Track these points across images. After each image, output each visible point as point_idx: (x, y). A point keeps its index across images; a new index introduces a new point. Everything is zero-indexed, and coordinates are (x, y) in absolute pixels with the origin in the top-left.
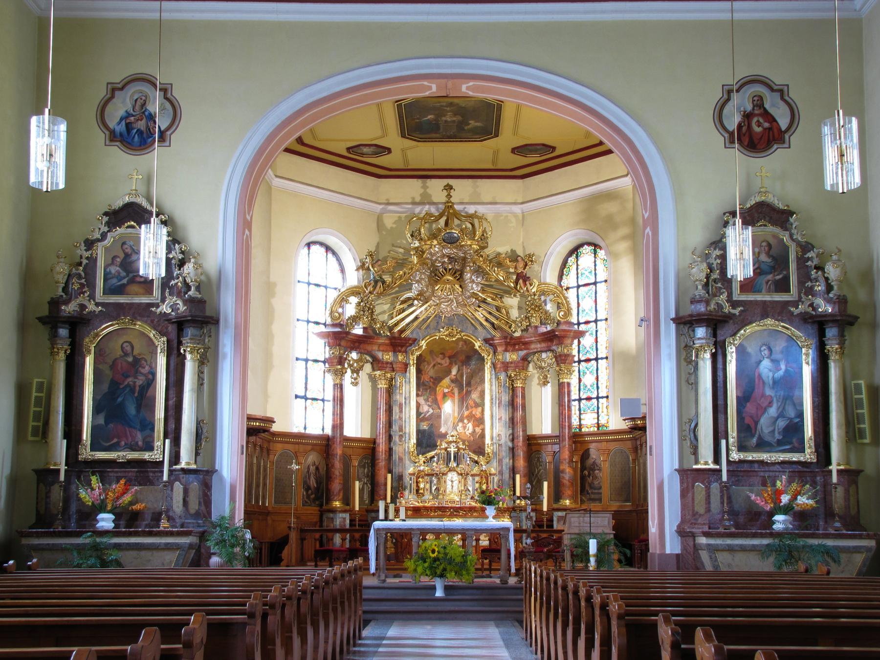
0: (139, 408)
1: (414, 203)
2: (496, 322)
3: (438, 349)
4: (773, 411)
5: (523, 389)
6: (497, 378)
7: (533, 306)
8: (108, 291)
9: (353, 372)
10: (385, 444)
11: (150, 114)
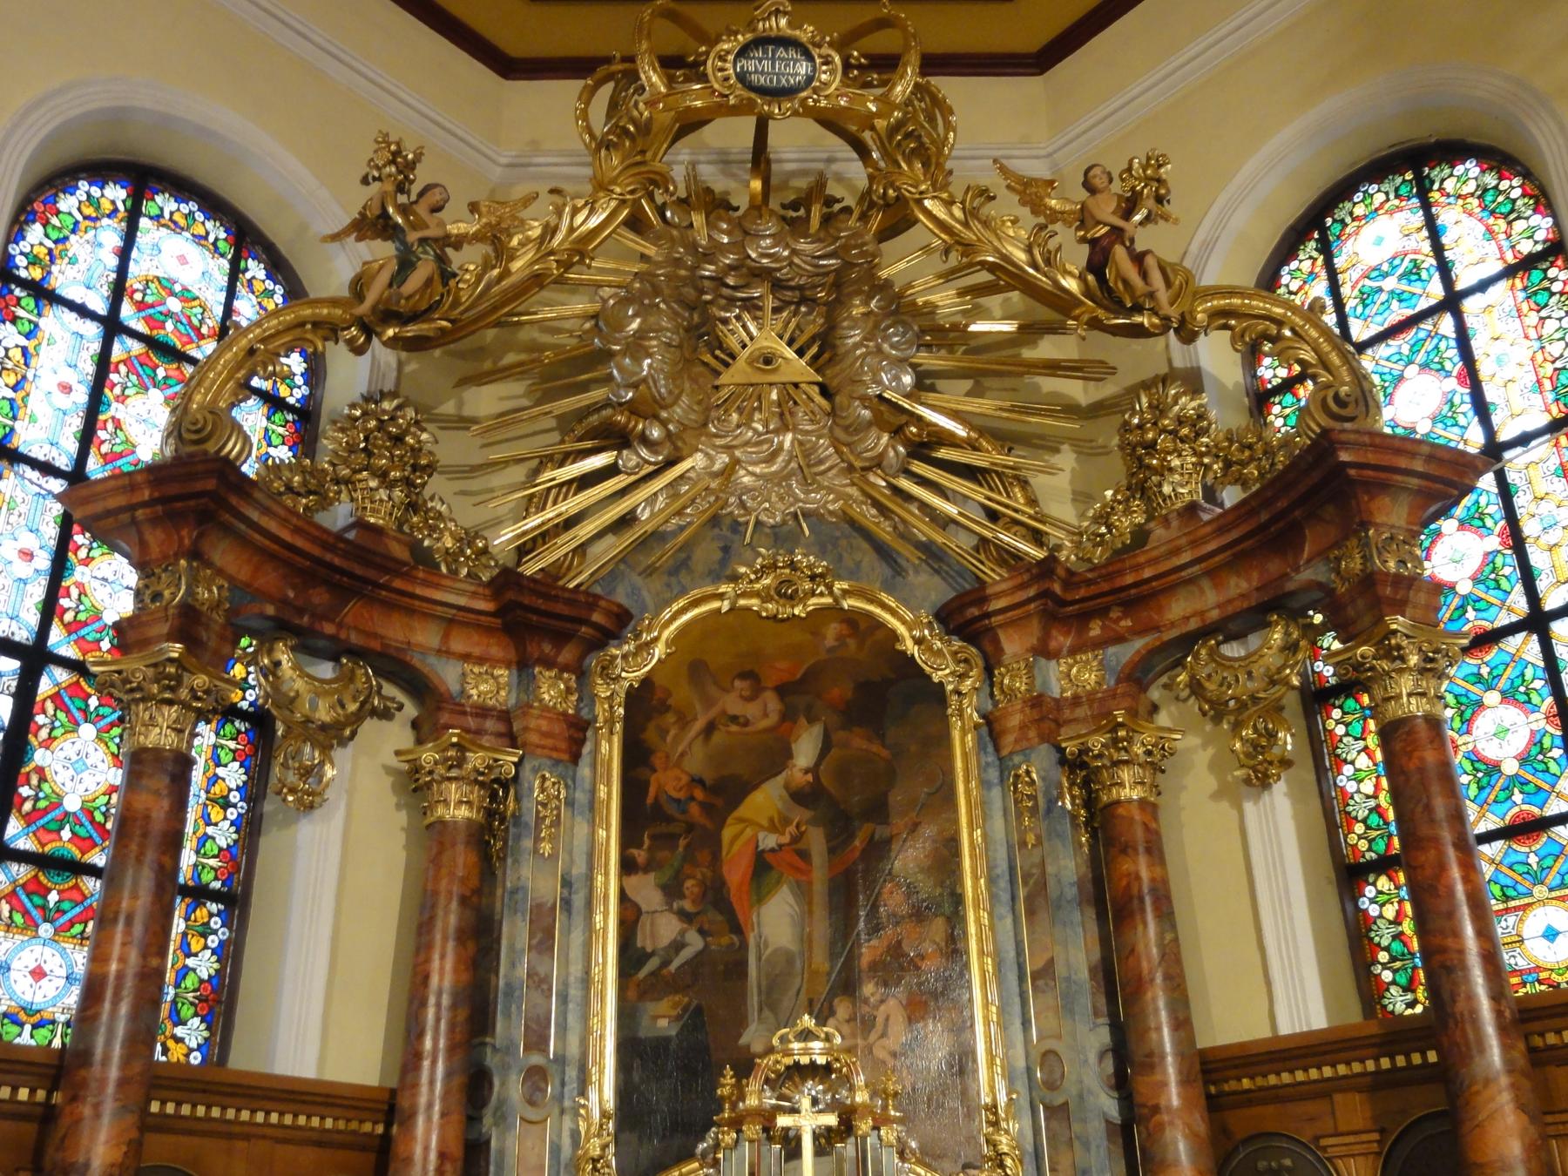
10: (443, 1115)
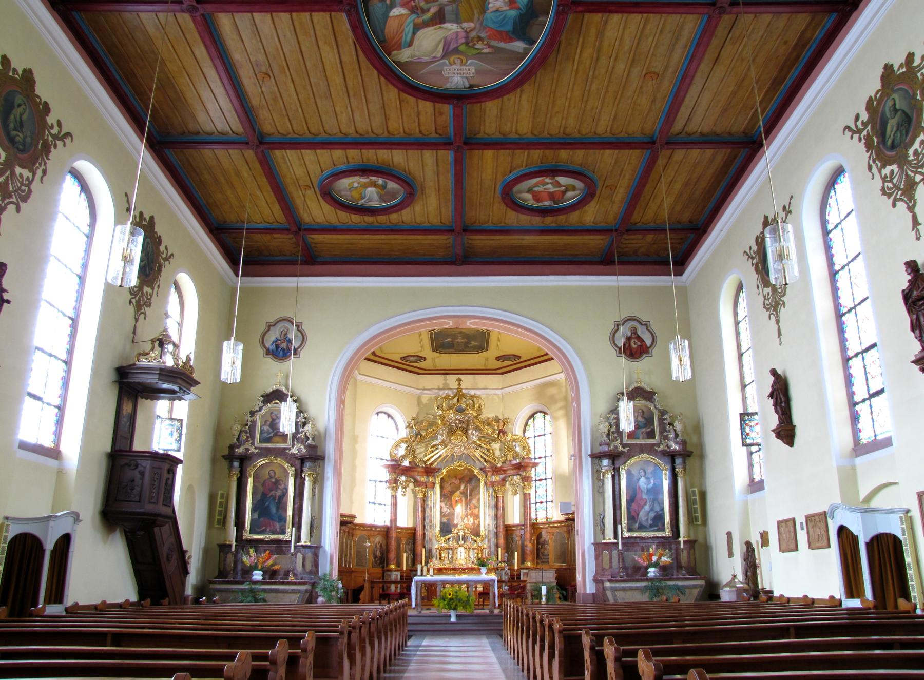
0: (278, 508)
1: (439, 389)
2: (486, 458)
3: (452, 474)
4: (647, 508)
5: (503, 497)
6: (488, 491)
7: (508, 448)
8: (263, 440)
9: (403, 488)
11: (289, 339)
